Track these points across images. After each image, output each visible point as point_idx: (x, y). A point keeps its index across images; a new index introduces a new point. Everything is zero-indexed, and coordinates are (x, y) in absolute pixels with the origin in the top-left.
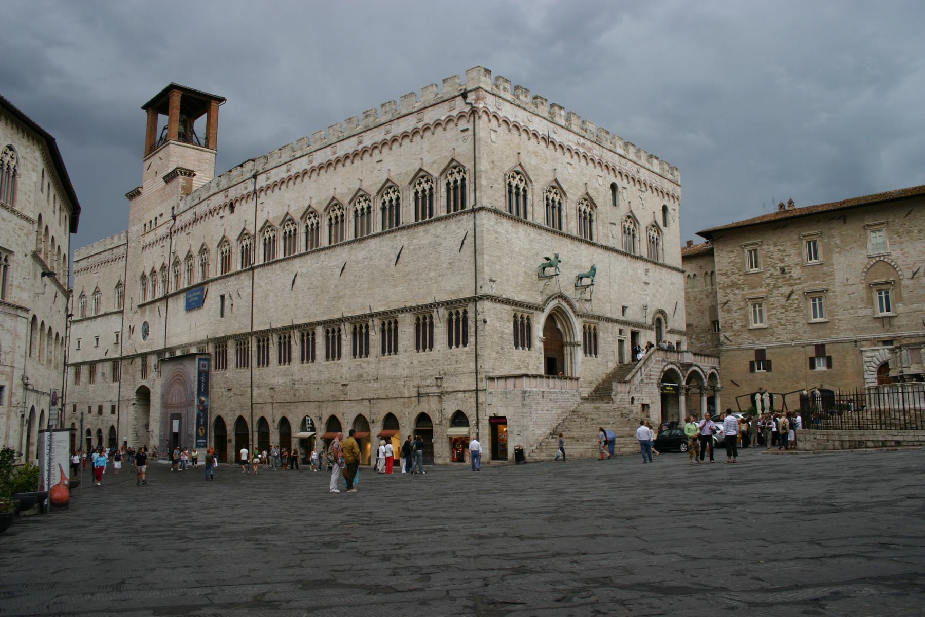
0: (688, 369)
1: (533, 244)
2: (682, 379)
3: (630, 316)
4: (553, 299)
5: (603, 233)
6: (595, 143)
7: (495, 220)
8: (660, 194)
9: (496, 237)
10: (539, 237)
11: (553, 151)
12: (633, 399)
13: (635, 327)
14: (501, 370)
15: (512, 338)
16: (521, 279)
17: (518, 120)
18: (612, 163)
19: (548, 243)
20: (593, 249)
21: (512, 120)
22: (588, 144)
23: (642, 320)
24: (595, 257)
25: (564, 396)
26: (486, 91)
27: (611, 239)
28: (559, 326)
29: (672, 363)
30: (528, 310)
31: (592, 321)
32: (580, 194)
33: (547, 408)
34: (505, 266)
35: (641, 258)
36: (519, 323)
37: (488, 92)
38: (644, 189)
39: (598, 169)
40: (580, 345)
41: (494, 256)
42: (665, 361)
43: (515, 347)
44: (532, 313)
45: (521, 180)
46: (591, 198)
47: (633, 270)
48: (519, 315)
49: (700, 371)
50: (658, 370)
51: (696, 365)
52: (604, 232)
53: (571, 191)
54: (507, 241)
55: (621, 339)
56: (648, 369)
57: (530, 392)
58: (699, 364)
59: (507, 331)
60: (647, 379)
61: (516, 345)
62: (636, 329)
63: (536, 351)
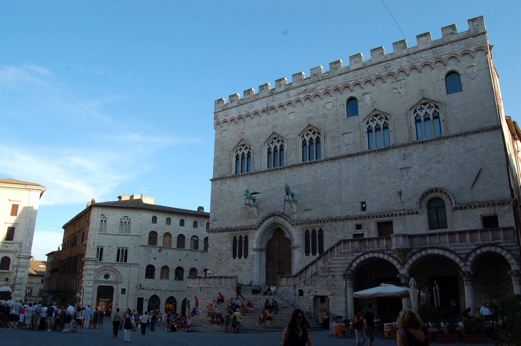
0: (411, 257)
1: (251, 186)
2: (398, 267)
3: (371, 208)
4: (266, 219)
5: (332, 147)
6: (319, 81)
7: (220, 183)
8: (438, 64)
9: (220, 193)
10: (256, 180)
11: (275, 114)
12: (301, 293)
13: (381, 216)
14: (218, 273)
15: (230, 253)
16: (239, 212)
17: (241, 113)
18: (343, 83)
19: (267, 180)
20: (315, 167)
21: (236, 116)
22: (312, 86)
23: (396, 208)
24: (319, 172)
25: (219, 290)
26: (218, 112)
27: (345, 147)
28: (287, 235)
29: (372, 252)
30: (244, 231)
31: (314, 224)
32: (302, 130)
33: (203, 298)
34: (227, 208)
35: (394, 147)
36: (238, 241)
37: (220, 112)
38: (402, 76)
39: (327, 99)
40: (296, 248)
41: (218, 205)
42: (358, 252)
43: (232, 258)
44: (248, 233)
45: (246, 148)
46: (314, 127)
47: (380, 163)
48: (238, 237)
49: (447, 254)
50: (346, 261)
51: (432, 248)
52: (334, 145)
53: (293, 132)
54: (229, 193)
55: (357, 233)
56: (326, 263)
57: (191, 287)
58: (448, 245)
59: (226, 248)
60: (323, 272)
61: (234, 257)
62: (387, 219)
63: (250, 258)
